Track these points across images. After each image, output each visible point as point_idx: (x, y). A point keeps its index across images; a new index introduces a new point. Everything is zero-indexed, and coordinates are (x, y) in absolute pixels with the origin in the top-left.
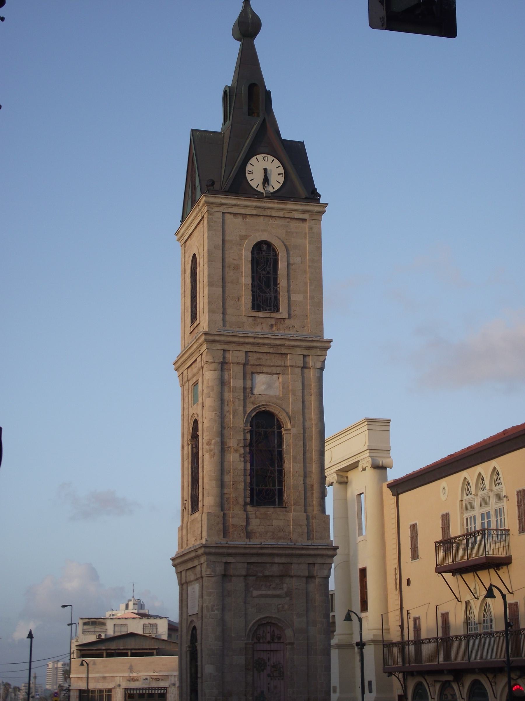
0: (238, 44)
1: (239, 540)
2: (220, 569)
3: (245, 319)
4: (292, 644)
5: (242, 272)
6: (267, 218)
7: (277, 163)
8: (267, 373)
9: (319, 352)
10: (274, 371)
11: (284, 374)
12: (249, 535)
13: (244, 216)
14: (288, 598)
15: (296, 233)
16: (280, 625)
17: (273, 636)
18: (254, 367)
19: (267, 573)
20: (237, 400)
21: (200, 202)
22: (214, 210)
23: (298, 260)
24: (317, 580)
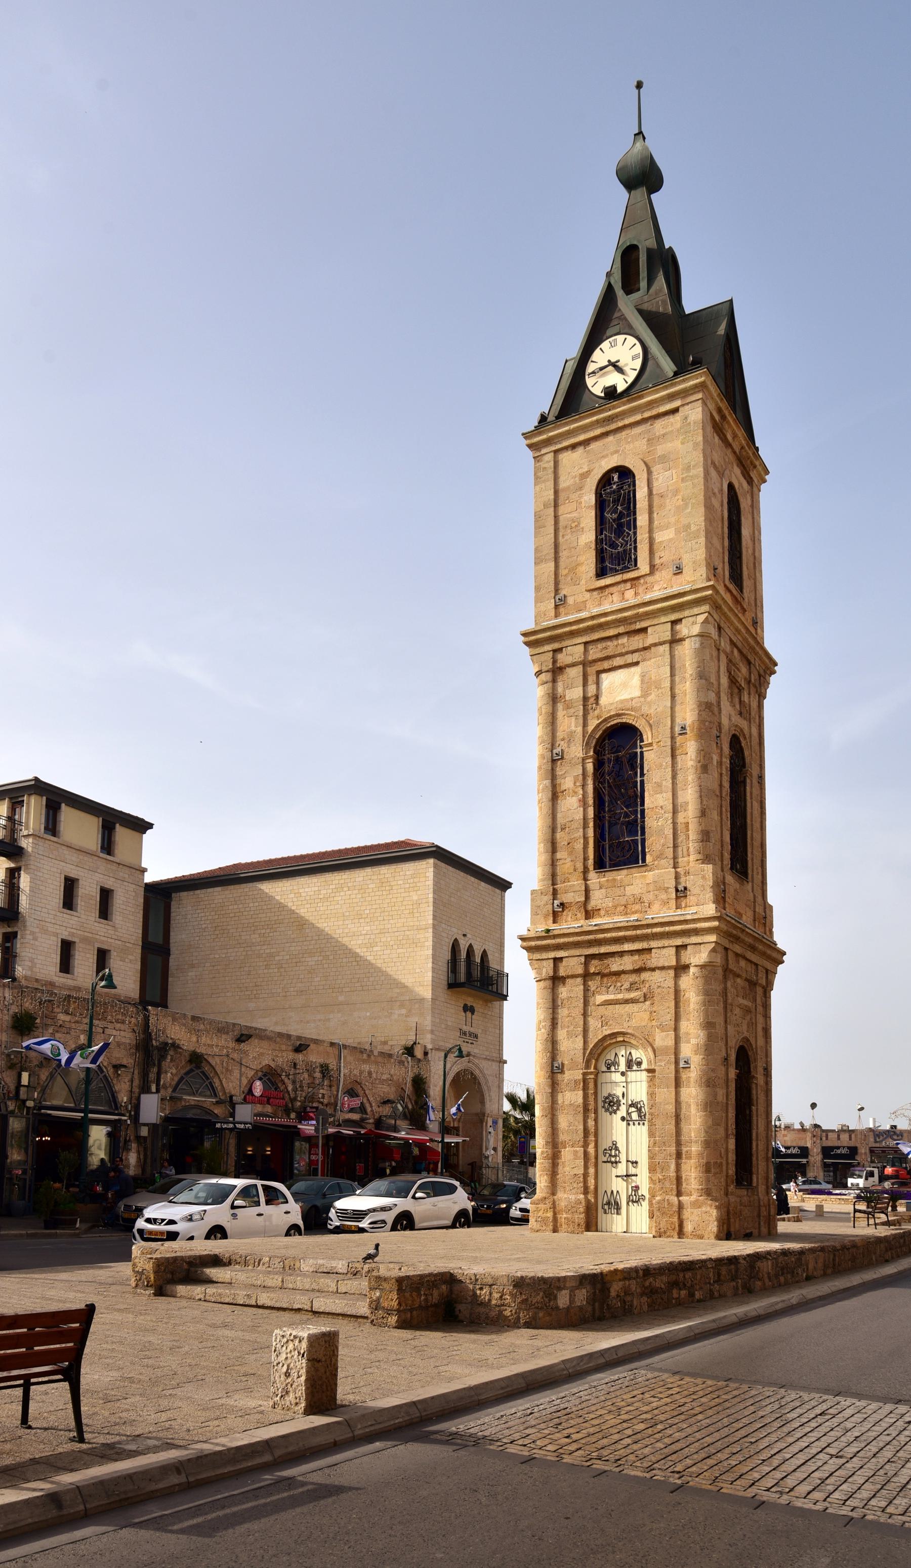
1: (572, 923)
2: (547, 969)
8: (620, 667)
11: (644, 660)
12: (588, 915)
14: (648, 1003)
19: (615, 968)
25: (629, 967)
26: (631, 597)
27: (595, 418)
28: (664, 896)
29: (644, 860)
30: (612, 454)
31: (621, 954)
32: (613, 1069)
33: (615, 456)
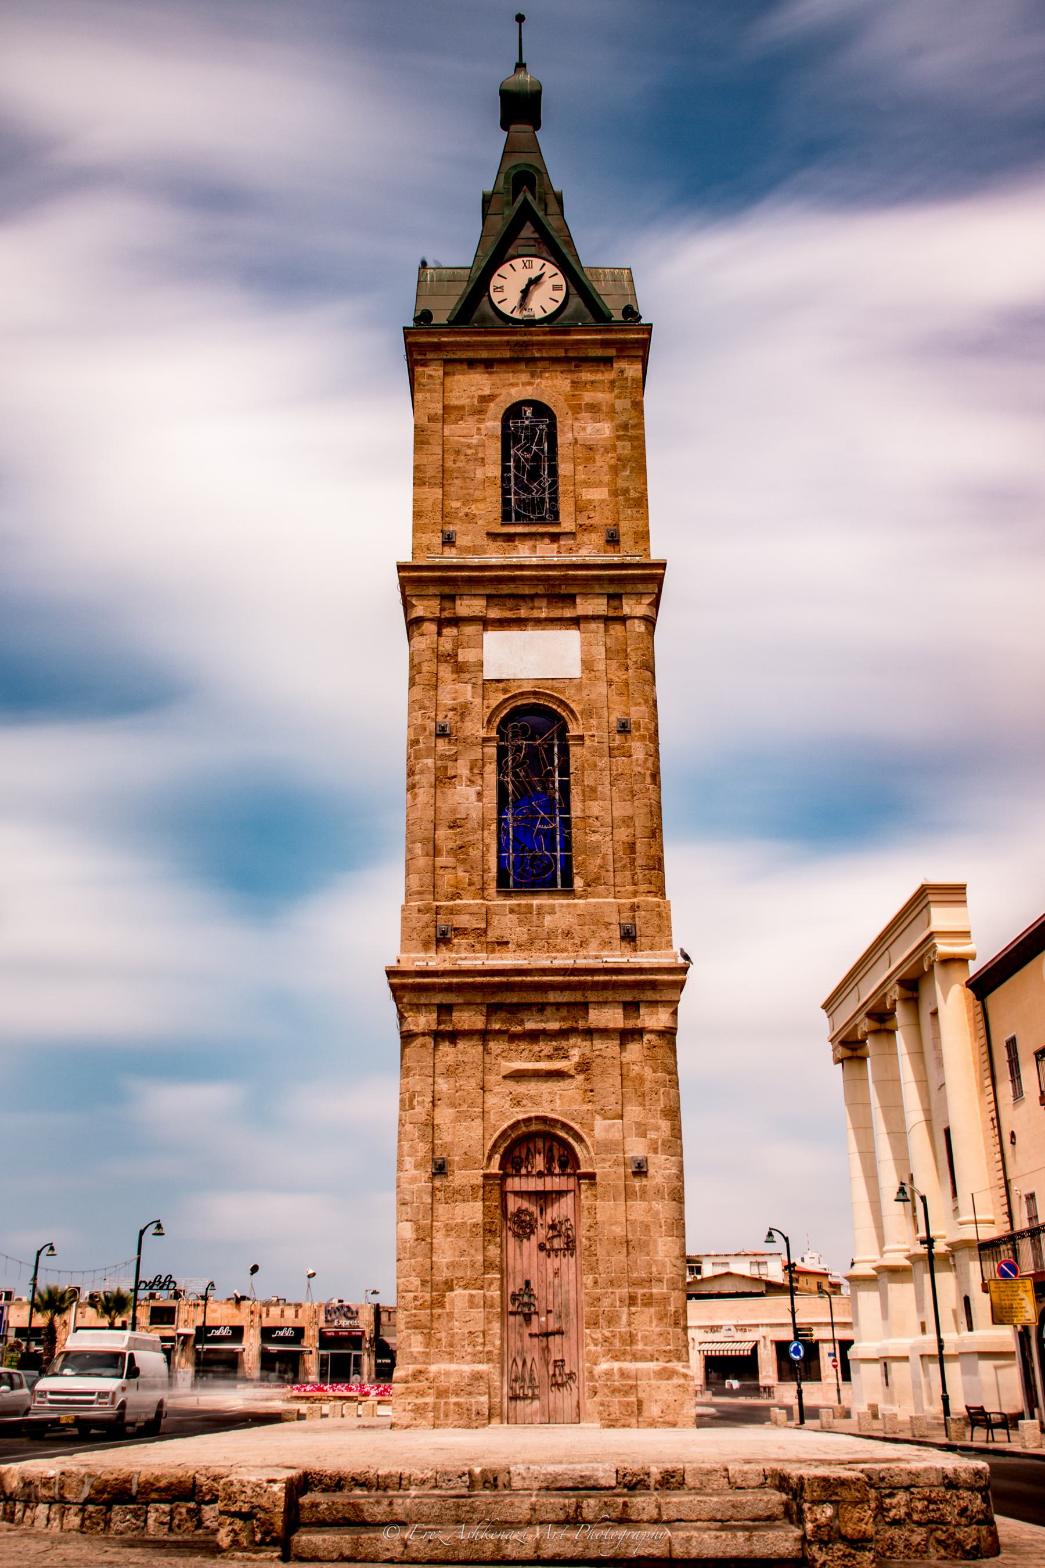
4: (592, 1176)
7: (550, 269)
9: (641, 588)
14: (580, 1078)
15: (592, 382)
16: (562, 1134)
17: (549, 1161)
19: (530, 1025)
20: (469, 687)
22: (428, 357)
24: (647, 1037)
25: (554, 1026)
26: (547, 553)
27: (505, 338)
28: (605, 934)
29: (568, 881)
30: (523, 384)
31: (541, 1007)
32: (523, 1171)
33: (529, 388)
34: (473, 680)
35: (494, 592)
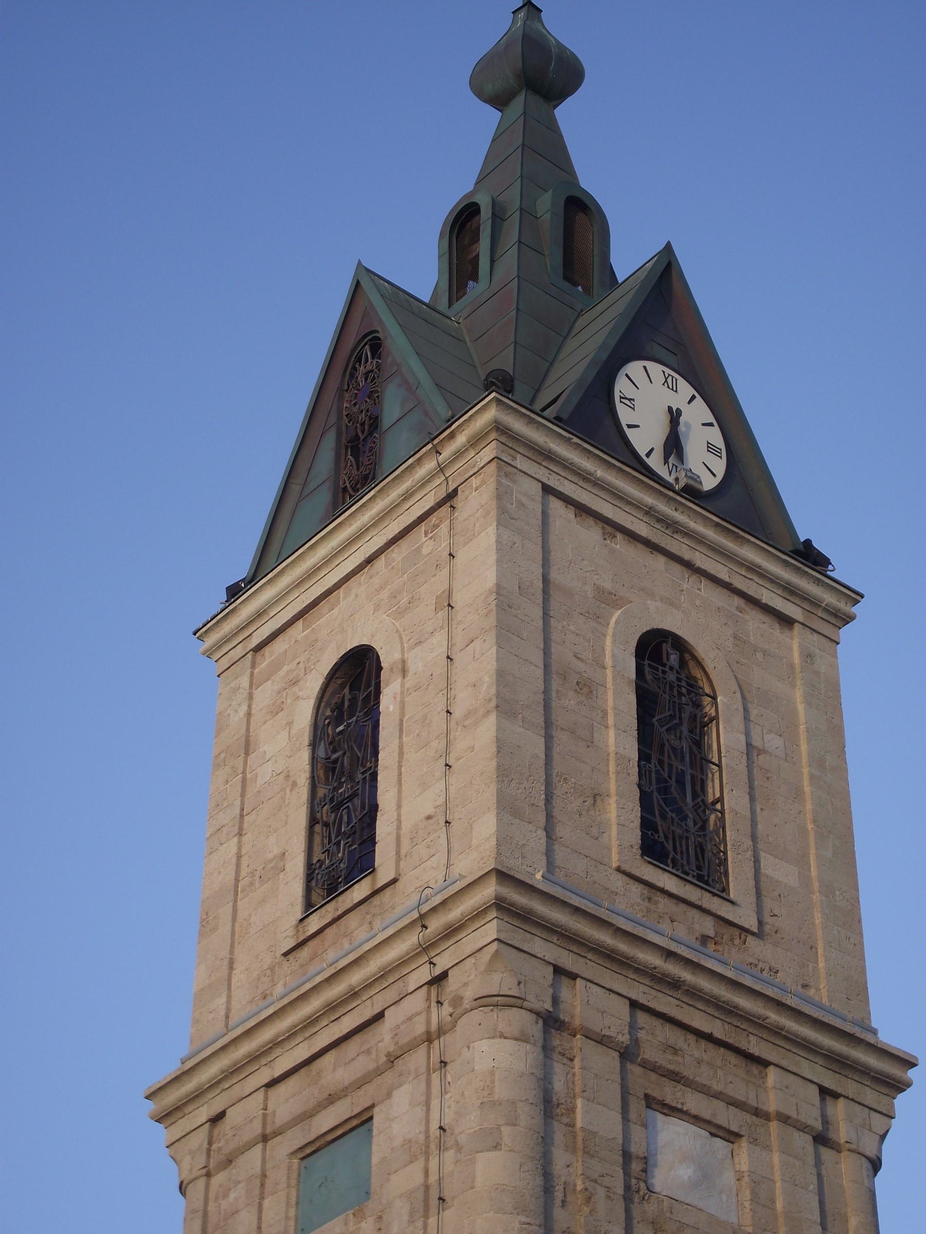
0: (492, 116)
3: (618, 882)
5: (605, 713)
6: (676, 568)
8: (696, 1120)
9: (870, 1096)
10: (721, 1120)
13: (612, 527)
18: (653, 1076)
20: (601, 1192)
21: (452, 436)
23: (774, 743)
34: (607, 1181)
35: (642, 1000)
